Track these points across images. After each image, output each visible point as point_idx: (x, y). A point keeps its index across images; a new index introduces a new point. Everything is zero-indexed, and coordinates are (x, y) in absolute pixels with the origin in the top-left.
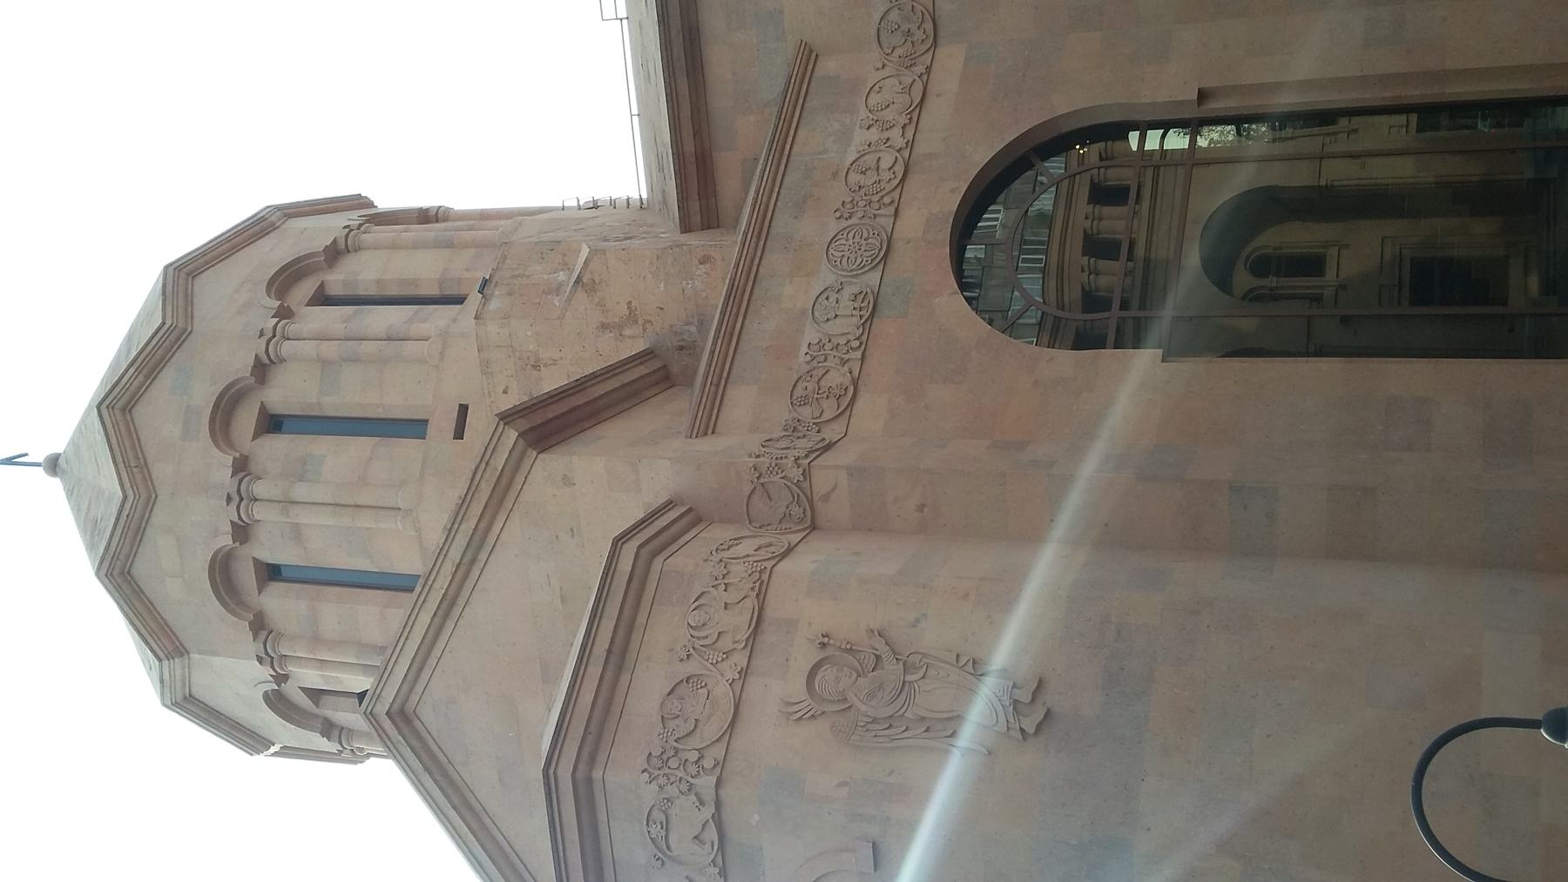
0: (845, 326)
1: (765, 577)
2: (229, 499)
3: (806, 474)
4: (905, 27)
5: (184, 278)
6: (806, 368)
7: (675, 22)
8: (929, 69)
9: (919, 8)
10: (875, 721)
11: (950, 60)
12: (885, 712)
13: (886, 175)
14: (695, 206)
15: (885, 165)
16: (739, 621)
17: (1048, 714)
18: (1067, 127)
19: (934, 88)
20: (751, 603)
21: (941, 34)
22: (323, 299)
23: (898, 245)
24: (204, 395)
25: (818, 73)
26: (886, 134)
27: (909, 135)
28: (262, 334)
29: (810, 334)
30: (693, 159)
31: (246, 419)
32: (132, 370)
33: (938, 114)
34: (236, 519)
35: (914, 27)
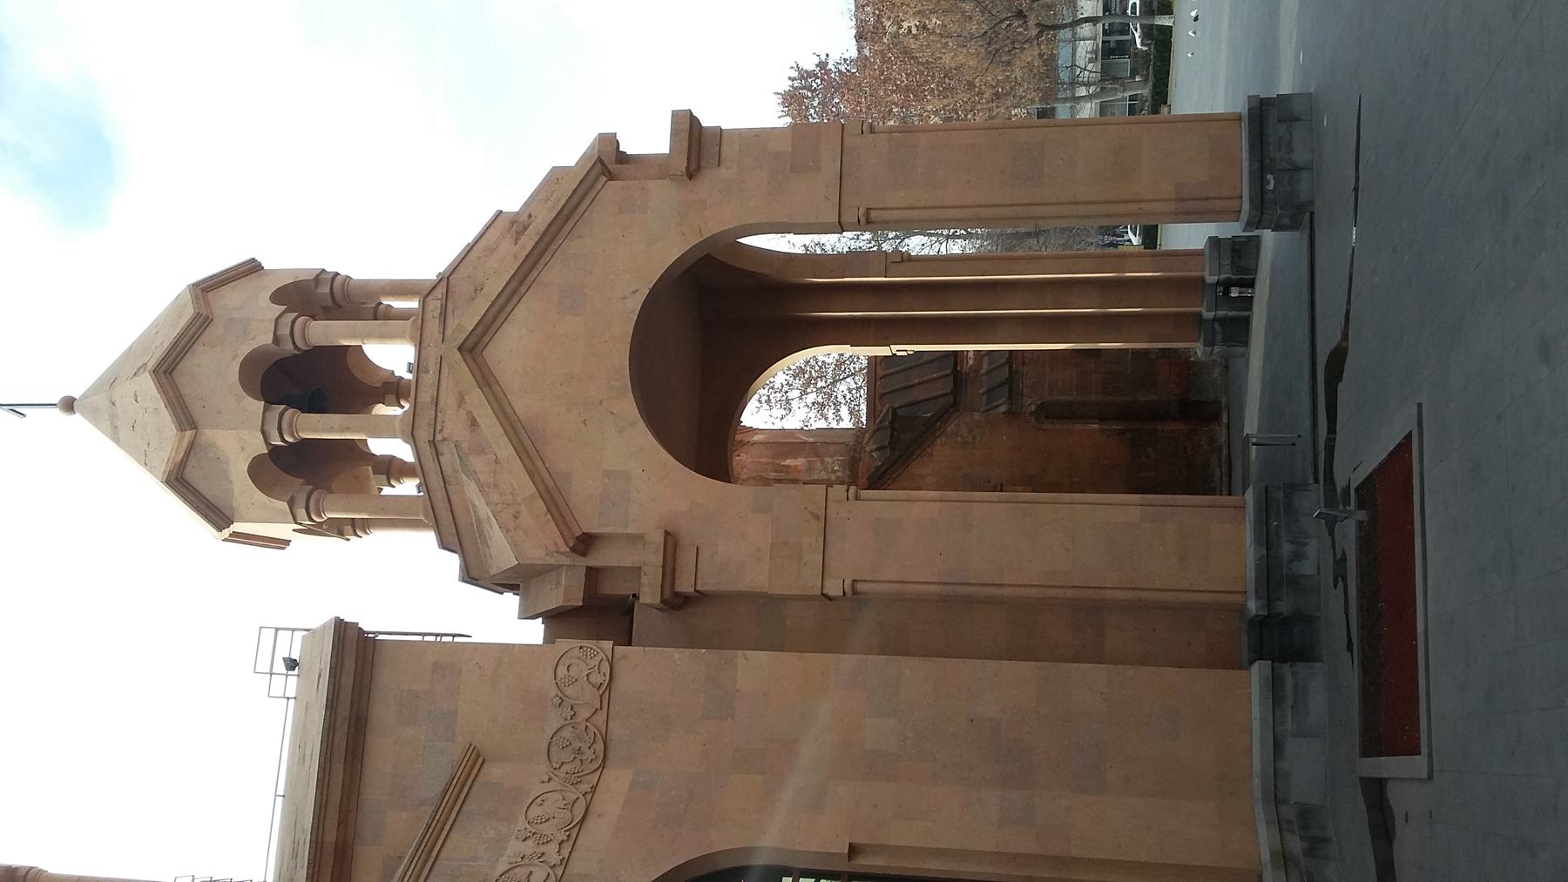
4: (577, 744)
7: (344, 710)
8: (594, 789)
11: (616, 784)
19: (595, 808)
21: (611, 755)
25: (481, 778)
26: (542, 849)
27: (565, 853)
30: (331, 851)
33: (597, 834)
35: (585, 747)
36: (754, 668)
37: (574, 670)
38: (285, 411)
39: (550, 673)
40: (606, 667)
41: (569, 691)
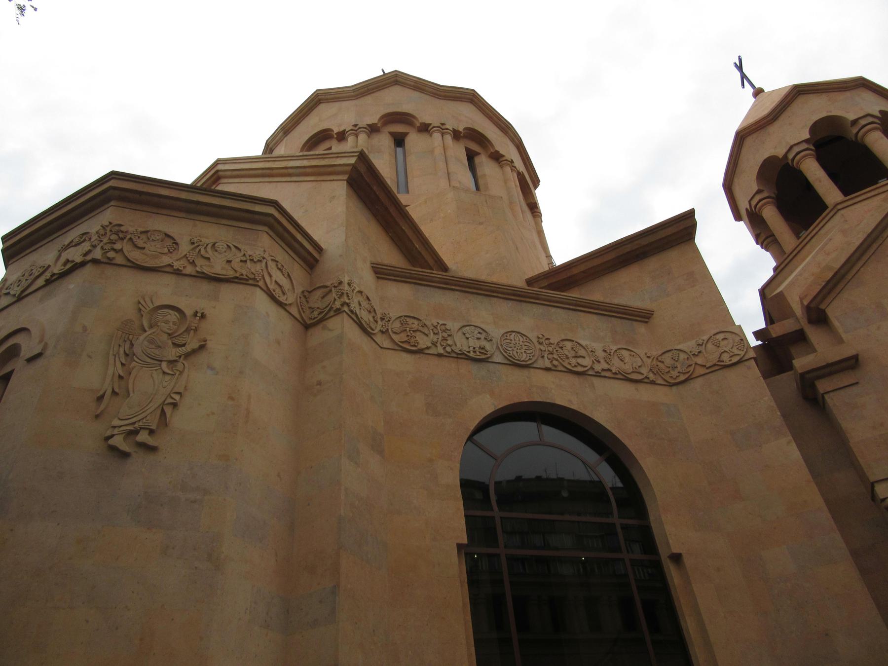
0: (461, 344)
1: (251, 282)
2: (355, 125)
3: (338, 311)
4: (677, 364)
5: (471, 98)
6: (427, 323)
8: (653, 383)
9: (691, 369)
10: (132, 345)
12: (137, 349)
13: (573, 361)
15: (580, 360)
16: (218, 267)
17: (125, 455)
18: (634, 472)
19: (641, 387)
20: (231, 274)
21: (680, 387)
22: (471, 156)
23: (525, 372)
24: (405, 108)
25: (635, 323)
26: (602, 361)
28: (443, 124)
29: (453, 326)
30: (569, 275)
31: (399, 128)
33: (622, 391)
36: (785, 452)
37: (725, 342)
38: (811, 150)
39: (716, 331)
40: (735, 359)
41: (710, 346)
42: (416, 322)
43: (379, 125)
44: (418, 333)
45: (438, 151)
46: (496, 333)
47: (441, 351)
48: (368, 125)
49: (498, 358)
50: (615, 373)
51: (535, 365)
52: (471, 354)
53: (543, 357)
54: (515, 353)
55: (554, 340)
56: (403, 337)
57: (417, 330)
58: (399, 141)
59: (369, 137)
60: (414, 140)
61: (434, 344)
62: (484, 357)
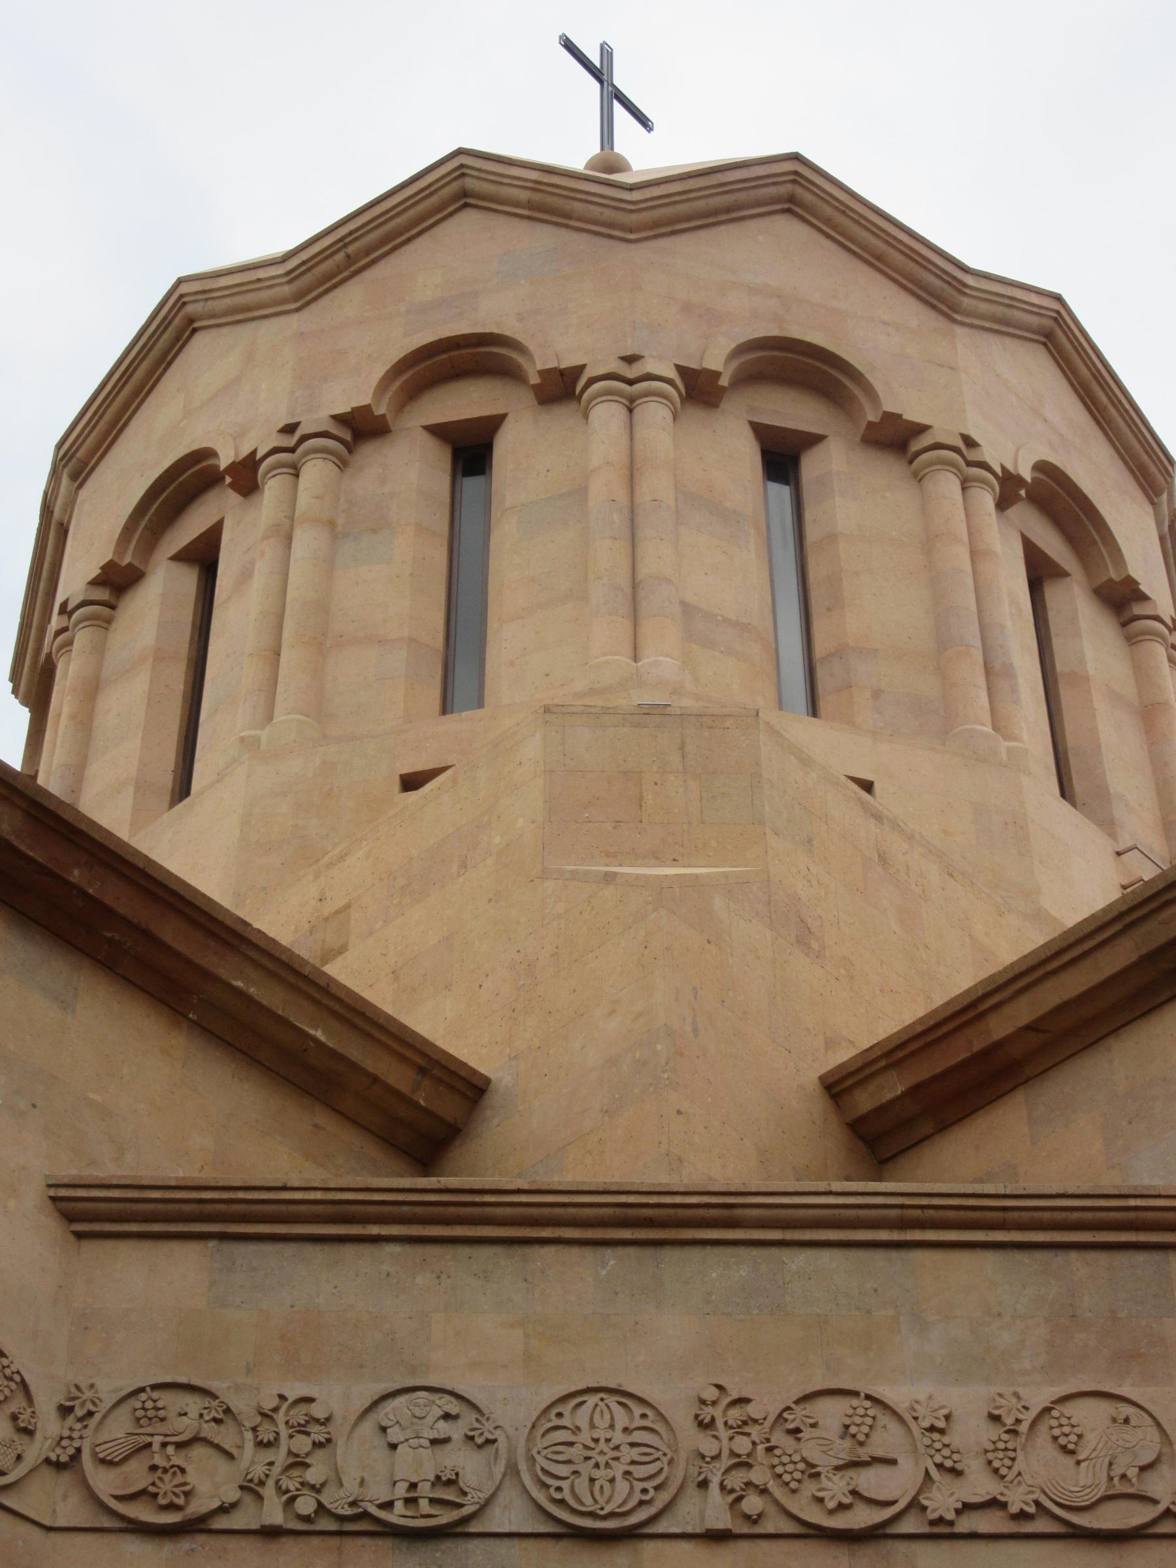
0: (364, 1471)
2: (289, 429)
6: (239, 1404)
13: (836, 1487)
14: (892, 1087)
15: (870, 1481)
24: (491, 314)
28: (630, 360)
29: (339, 1397)
30: (978, 1045)
31: (463, 402)
32: (534, 175)
34: (259, 455)
42: (193, 1404)
43: (380, 410)
44: (198, 1451)
45: (605, 488)
46: (513, 1404)
47: (274, 1514)
48: (339, 419)
49: (510, 1515)
50: (1022, 1516)
51: (661, 1527)
52: (397, 1516)
53: (704, 1484)
54: (582, 1484)
55: (765, 1406)
56: (136, 1475)
57: (196, 1439)
58: (471, 451)
59: (343, 464)
60: (528, 448)
61: (251, 1489)
62: (446, 1517)
